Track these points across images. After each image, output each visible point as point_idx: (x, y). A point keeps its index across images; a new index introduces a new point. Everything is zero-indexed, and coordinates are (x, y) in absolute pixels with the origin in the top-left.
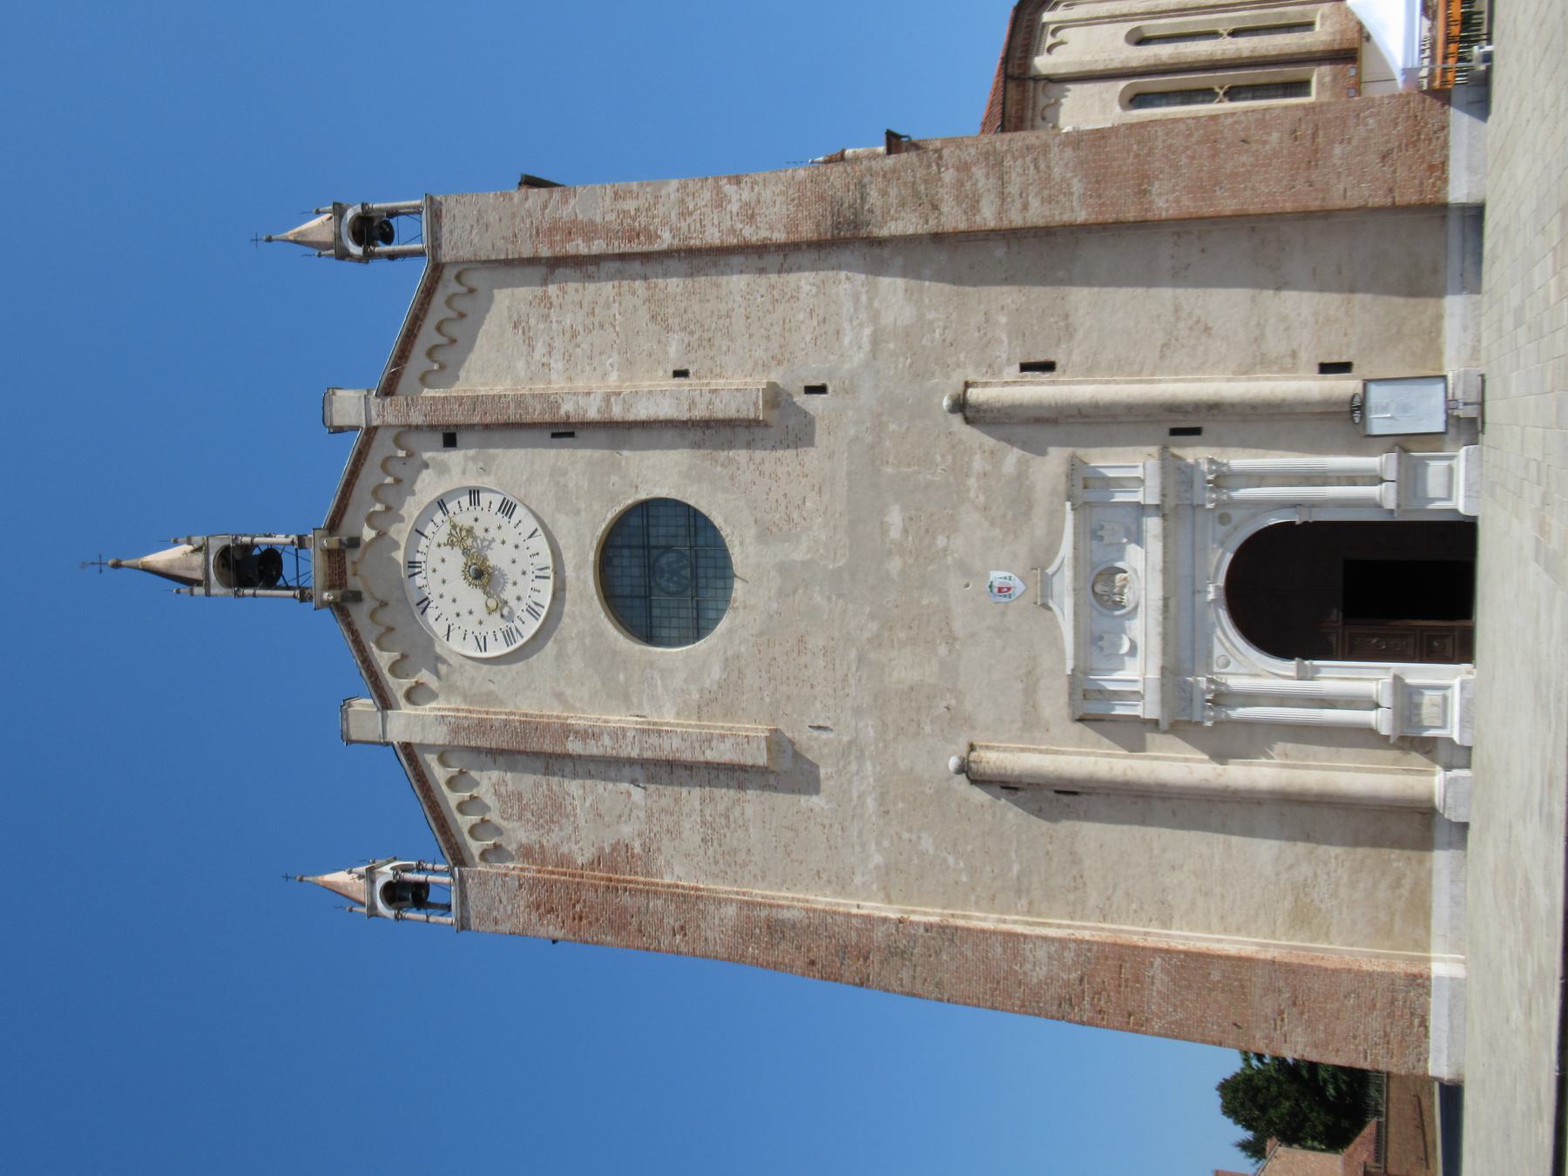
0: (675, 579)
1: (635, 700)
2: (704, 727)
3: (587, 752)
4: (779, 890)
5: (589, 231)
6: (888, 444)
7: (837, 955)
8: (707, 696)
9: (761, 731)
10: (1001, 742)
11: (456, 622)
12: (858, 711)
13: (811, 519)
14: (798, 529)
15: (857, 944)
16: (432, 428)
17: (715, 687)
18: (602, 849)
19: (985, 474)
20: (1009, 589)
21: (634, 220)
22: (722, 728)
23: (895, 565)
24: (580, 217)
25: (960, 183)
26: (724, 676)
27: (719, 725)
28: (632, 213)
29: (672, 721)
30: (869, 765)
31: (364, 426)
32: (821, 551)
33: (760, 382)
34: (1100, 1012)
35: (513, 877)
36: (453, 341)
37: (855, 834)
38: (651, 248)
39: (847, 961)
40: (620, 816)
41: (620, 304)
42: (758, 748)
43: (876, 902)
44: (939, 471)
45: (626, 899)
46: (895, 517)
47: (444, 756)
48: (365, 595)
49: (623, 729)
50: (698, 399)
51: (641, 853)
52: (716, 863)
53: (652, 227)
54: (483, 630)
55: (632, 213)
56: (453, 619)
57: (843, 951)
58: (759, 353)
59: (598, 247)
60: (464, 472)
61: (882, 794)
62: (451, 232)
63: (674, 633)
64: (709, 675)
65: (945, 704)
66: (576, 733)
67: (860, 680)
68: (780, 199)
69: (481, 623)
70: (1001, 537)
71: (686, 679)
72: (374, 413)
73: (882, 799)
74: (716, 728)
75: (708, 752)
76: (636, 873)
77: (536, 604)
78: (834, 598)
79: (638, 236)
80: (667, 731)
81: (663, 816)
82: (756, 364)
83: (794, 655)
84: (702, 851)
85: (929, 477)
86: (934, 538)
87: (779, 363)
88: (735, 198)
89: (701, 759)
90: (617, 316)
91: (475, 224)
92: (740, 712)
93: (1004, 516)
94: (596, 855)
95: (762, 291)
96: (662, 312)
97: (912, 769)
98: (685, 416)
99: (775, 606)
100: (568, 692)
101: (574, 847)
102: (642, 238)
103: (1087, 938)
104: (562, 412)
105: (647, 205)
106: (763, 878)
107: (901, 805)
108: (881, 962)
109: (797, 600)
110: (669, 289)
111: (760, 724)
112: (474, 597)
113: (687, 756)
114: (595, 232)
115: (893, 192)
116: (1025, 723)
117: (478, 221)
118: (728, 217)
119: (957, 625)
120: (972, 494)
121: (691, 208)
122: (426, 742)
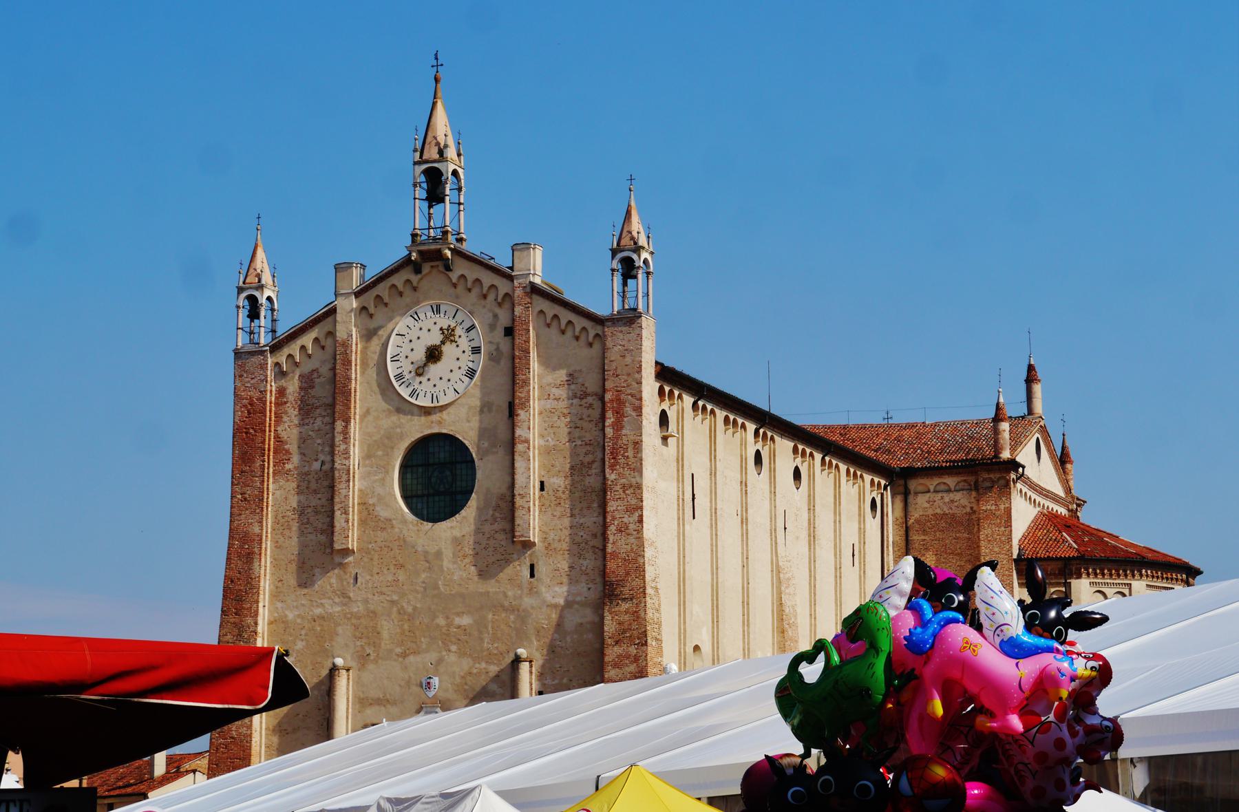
0: (438, 482)
1: (367, 462)
2: (353, 507)
3: (336, 434)
4: (271, 557)
5: (618, 426)
6: (503, 615)
7: (237, 596)
8: (371, 508)
9: (353, 543)
10: (353, 686)
11: (407, 341)
12: (366, 601)
13: (465, 570)
14: (459, 562)
15: (244, 608)
16: (513, 320)
17: (376, 514)
18: (287, 444)
19: (487, 673)
20: (429, 688)
21: (623, 456)
22: (353, 520)
23: (441, 621)
24: (625, 419)
25: (628, 656)
26: (382, 519)
27: (354, 516)
28: (626, 454)
29: (356, 487)
30: (338, 609)
31: (513, 274)
32: (448, 577)
33: (534, 536)
34: (217, 749)
35: (266, 386)
36: (563, 332)
37: (303, 602)
38: (607, 467)
39: (234, 602)
40: (304, 455)
41: (581, 445)
42: (342, 544)
43: (268, 617)
44: (490, 646)
45: (258, 463)
46: (466, 621)
47: (331, 334)
48: (419, 276)
49: (349, 458)
50: (525, 499)
51: (286, 469)
52: (283, 517)
53: (618, 467)
54: (402, 359)
55: (626, 454)
56: (408, 337)
57: (240, 600)
58: (552, 536)
59: (609, 431)
60: (490, 342)
61: (323, 617)
62: (622, 332)
63: (409, 482)
64: (382, 509)
65: (371, 653)
66: (346, 427)
67: (382, 602)
68: (629, 547)
69: (412, 350)
70: (456, 682)
71: (379, 494)
72: (521, 281)
73: (322, 618)
74: (353, 515)
75: (339, 512)
76: (274, 466)
77: (418, 394)
78: (424, 585)
79: (614, 458)
80: (349, 486)
81: (306, 482)
82: (546, 533)
83: (394, 562)
84: (289, 508)
85: (486, 641)
86: (455, 644)
87: (547, 548)
88: (631, 520)
89: (336, 508)
90: (574, 443)
91: (625, 348)
92: (363, 529)
93: (466, 684)
94: (282, 439)
95: (585, 536)
96: (575, 473)
97: (338, 635)
98: (516, 492)
99: (419, 549)
100: (370, 418)
101: (286, 425)
102: (613, 461)
103: (253, 739)
104: (520, 412)
105: (630, 463)
106: (276, 547)
107: (319, 629)
108: (234, 623)
109: (422, 563)
110: (588, 477)
111: (357, 542)
112: (420, 355)
113: (337, 499)
114: (617, 430)
115: (627, 617)
116: (363, 699)
117: (627, 350)
118: (622, 516)
119: (412, 658)
120: (477, 665)
121: (627, 492)
122: (337, 324)
